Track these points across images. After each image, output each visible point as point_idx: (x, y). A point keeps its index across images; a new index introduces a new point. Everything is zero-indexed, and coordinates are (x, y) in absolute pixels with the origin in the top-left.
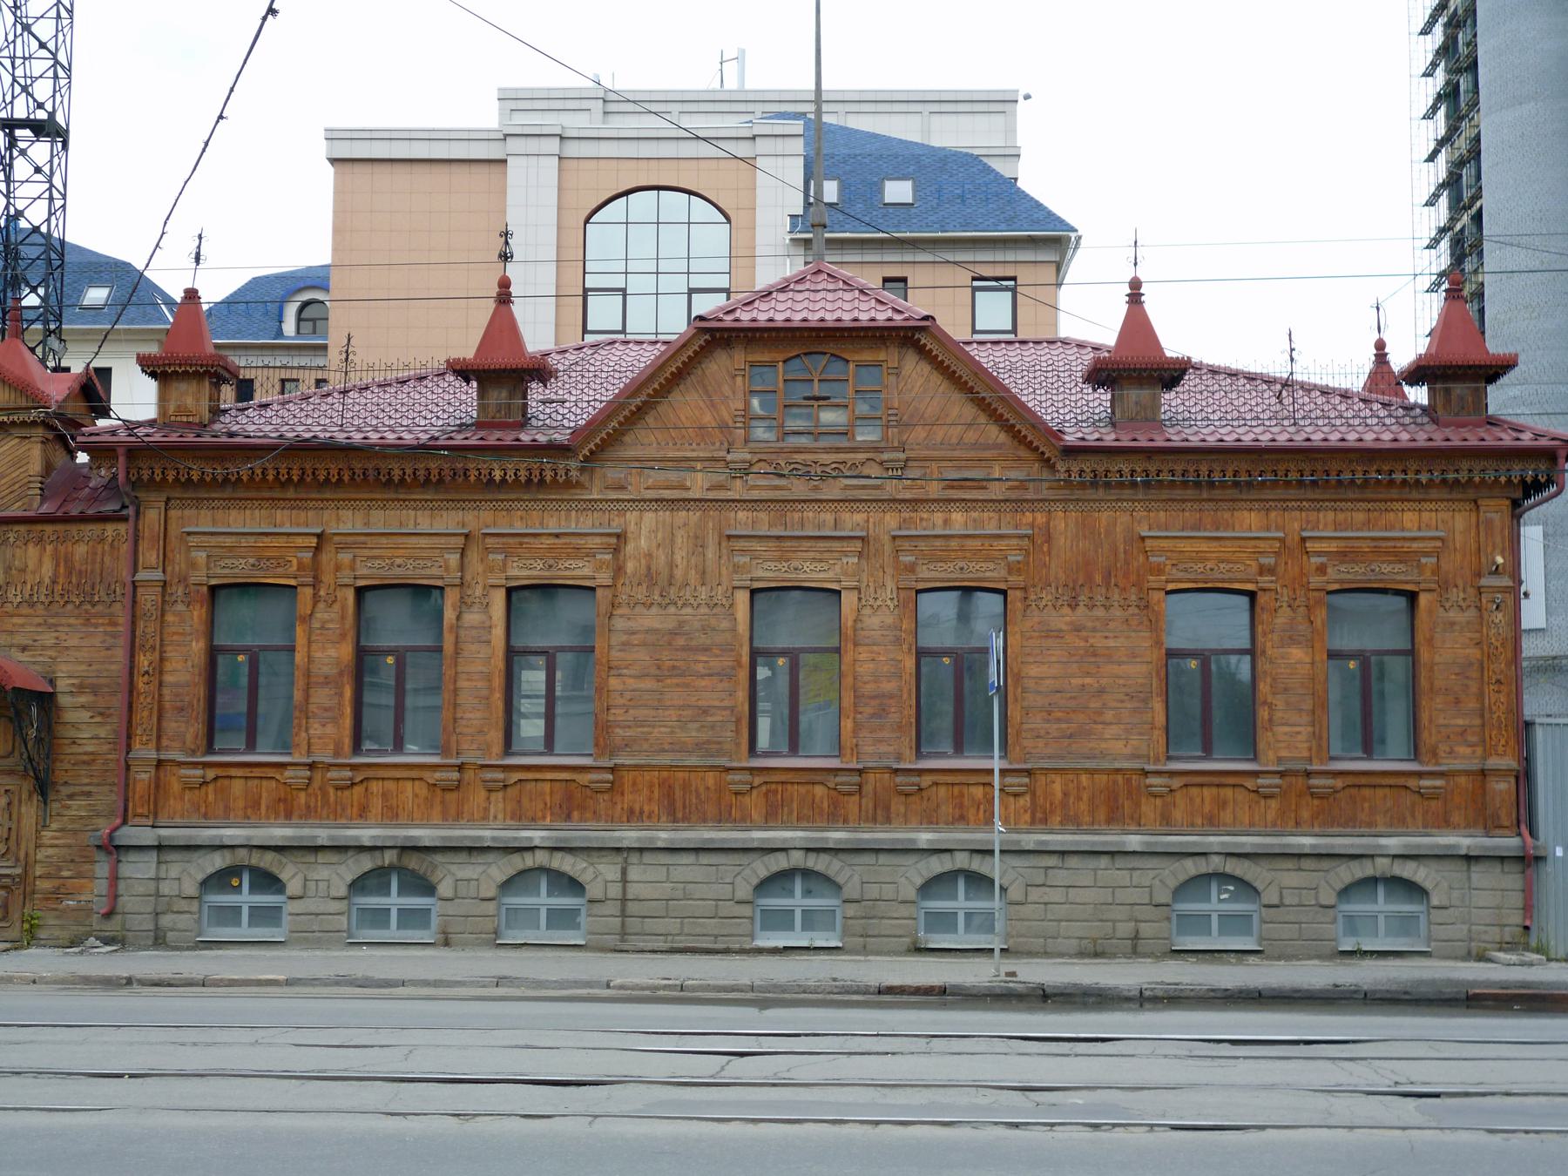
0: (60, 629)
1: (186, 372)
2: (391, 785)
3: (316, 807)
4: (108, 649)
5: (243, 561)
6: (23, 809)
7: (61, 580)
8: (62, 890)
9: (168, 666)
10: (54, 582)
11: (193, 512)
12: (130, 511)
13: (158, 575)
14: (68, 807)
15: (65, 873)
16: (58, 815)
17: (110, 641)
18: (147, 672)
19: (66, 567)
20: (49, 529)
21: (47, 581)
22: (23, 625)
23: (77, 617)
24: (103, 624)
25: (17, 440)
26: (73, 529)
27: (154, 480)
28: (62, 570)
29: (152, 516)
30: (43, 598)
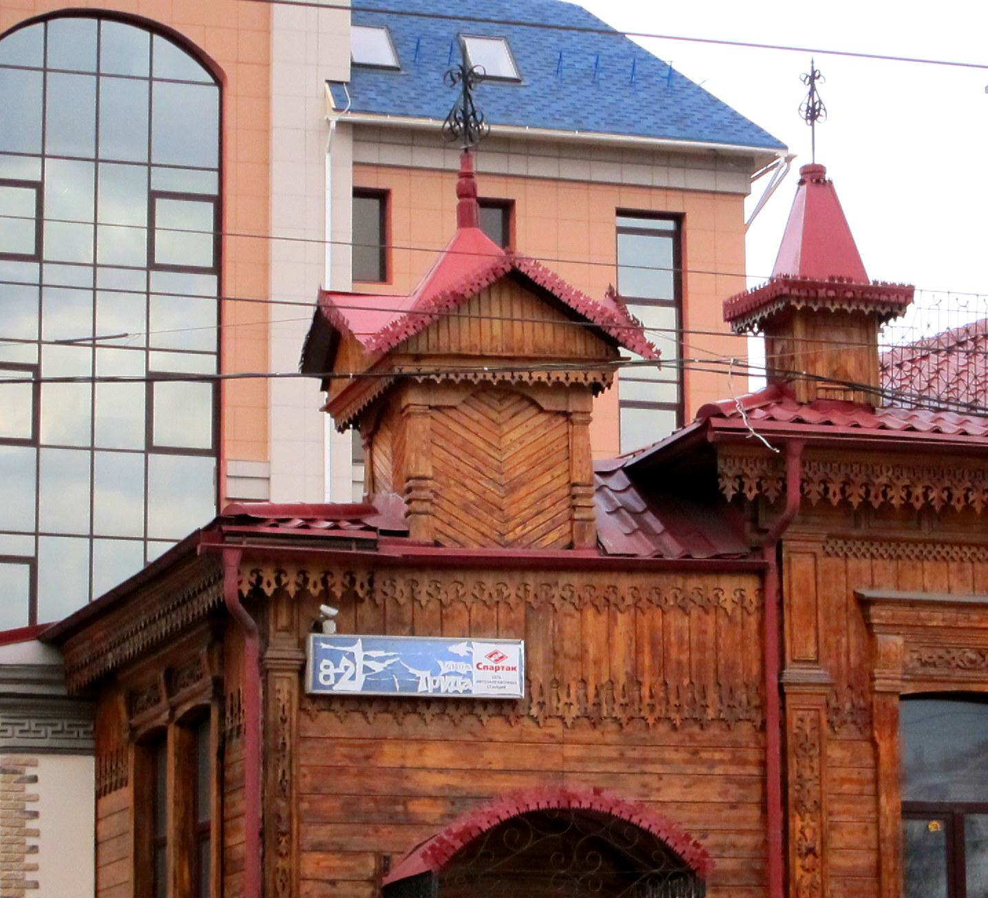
0: (648, 768)
1: (841, 313)
4: (733, 806)
5: (956, 653)
7: (647, 680)
9: (837, 840)
10: (635, 679)
11: (865, 563)
12: (770, 556)
13: (818, 674)
17: (735, 792)
18: (811, 851)
19: (653, 657)
20: (625, 583)
21: (622, 679)
22: (580, 760)
23: (676, 748)
24: (722, 762)
25: (542, 418)
26: (671, 585)
27: (829, 501)
28: (647, 660)
29: (800, 567)
30: (618, 713)
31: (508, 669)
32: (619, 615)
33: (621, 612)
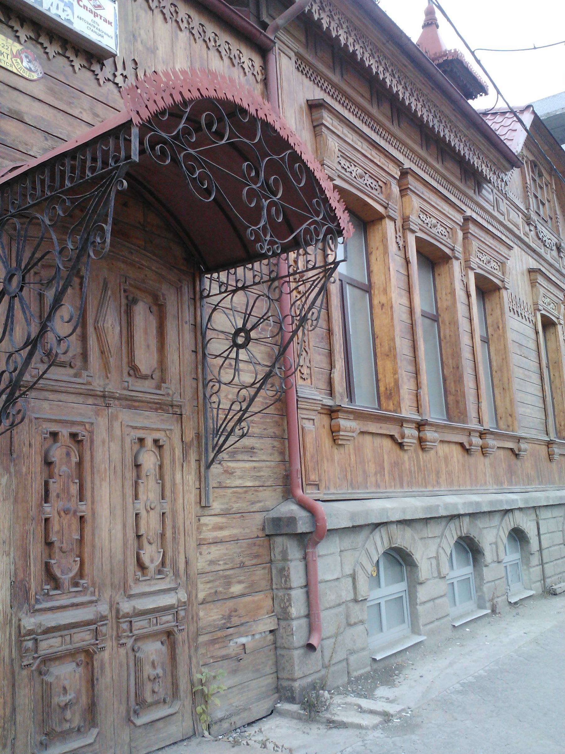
2: (446, 447)
3: (415, 472)
6: (178, 476)
8: (235, 620)
14: (229, 473)
15: (236, 589)
16: (220, 486)
31: (105, 21)
32: (179, 32)
33: (181, 30)
